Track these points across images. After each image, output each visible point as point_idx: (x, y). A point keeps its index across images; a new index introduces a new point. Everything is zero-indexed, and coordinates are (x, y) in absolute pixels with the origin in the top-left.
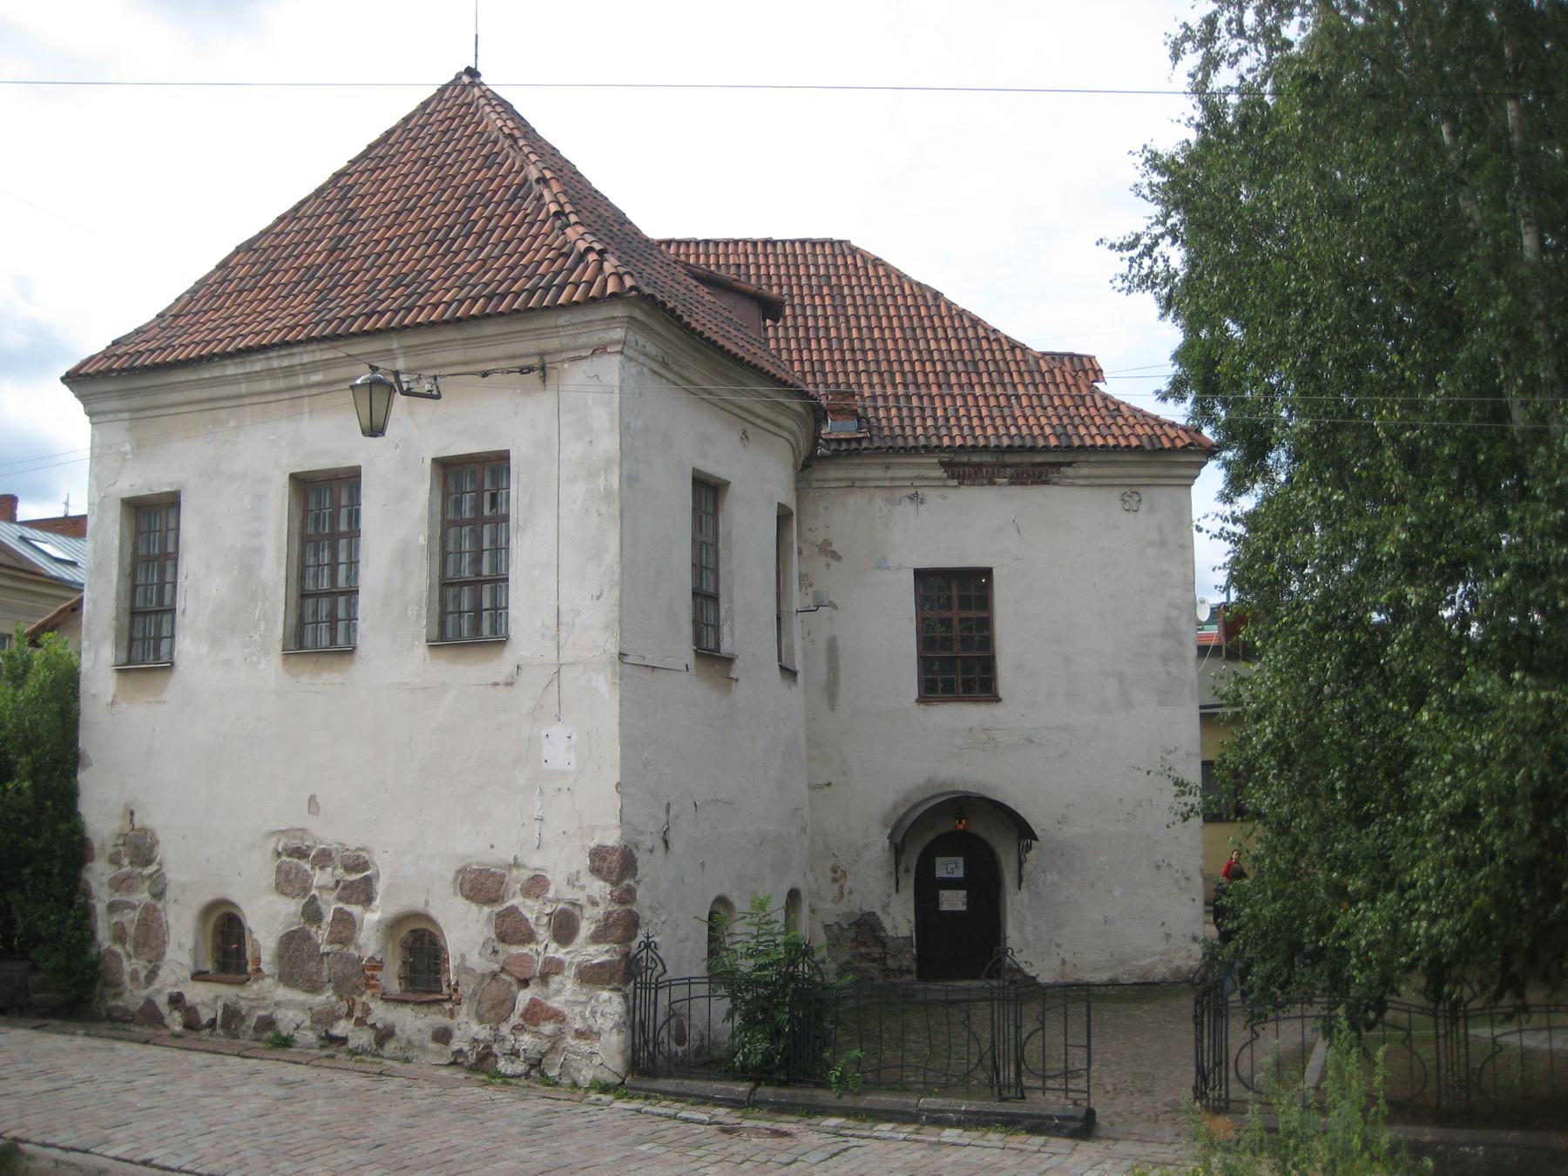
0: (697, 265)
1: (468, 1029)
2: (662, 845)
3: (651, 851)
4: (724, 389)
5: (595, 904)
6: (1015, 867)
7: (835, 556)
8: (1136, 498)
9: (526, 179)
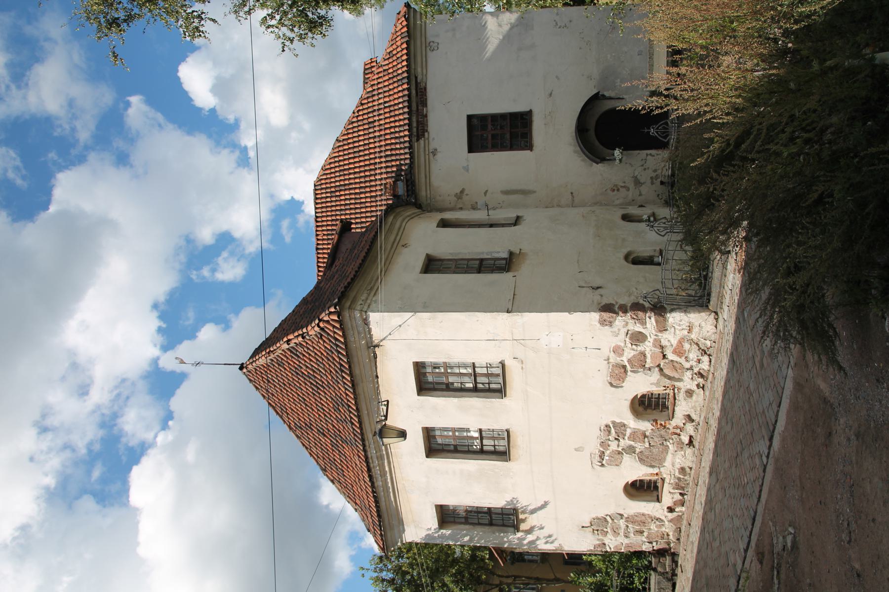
0: (327, 263)
1: (688, 382)
2: (599, 290)
3: (602, 296)
4: (381, 257)
5: (627, 324)
6: (613, 101)
7: (462, 192)
9: (288, 349)
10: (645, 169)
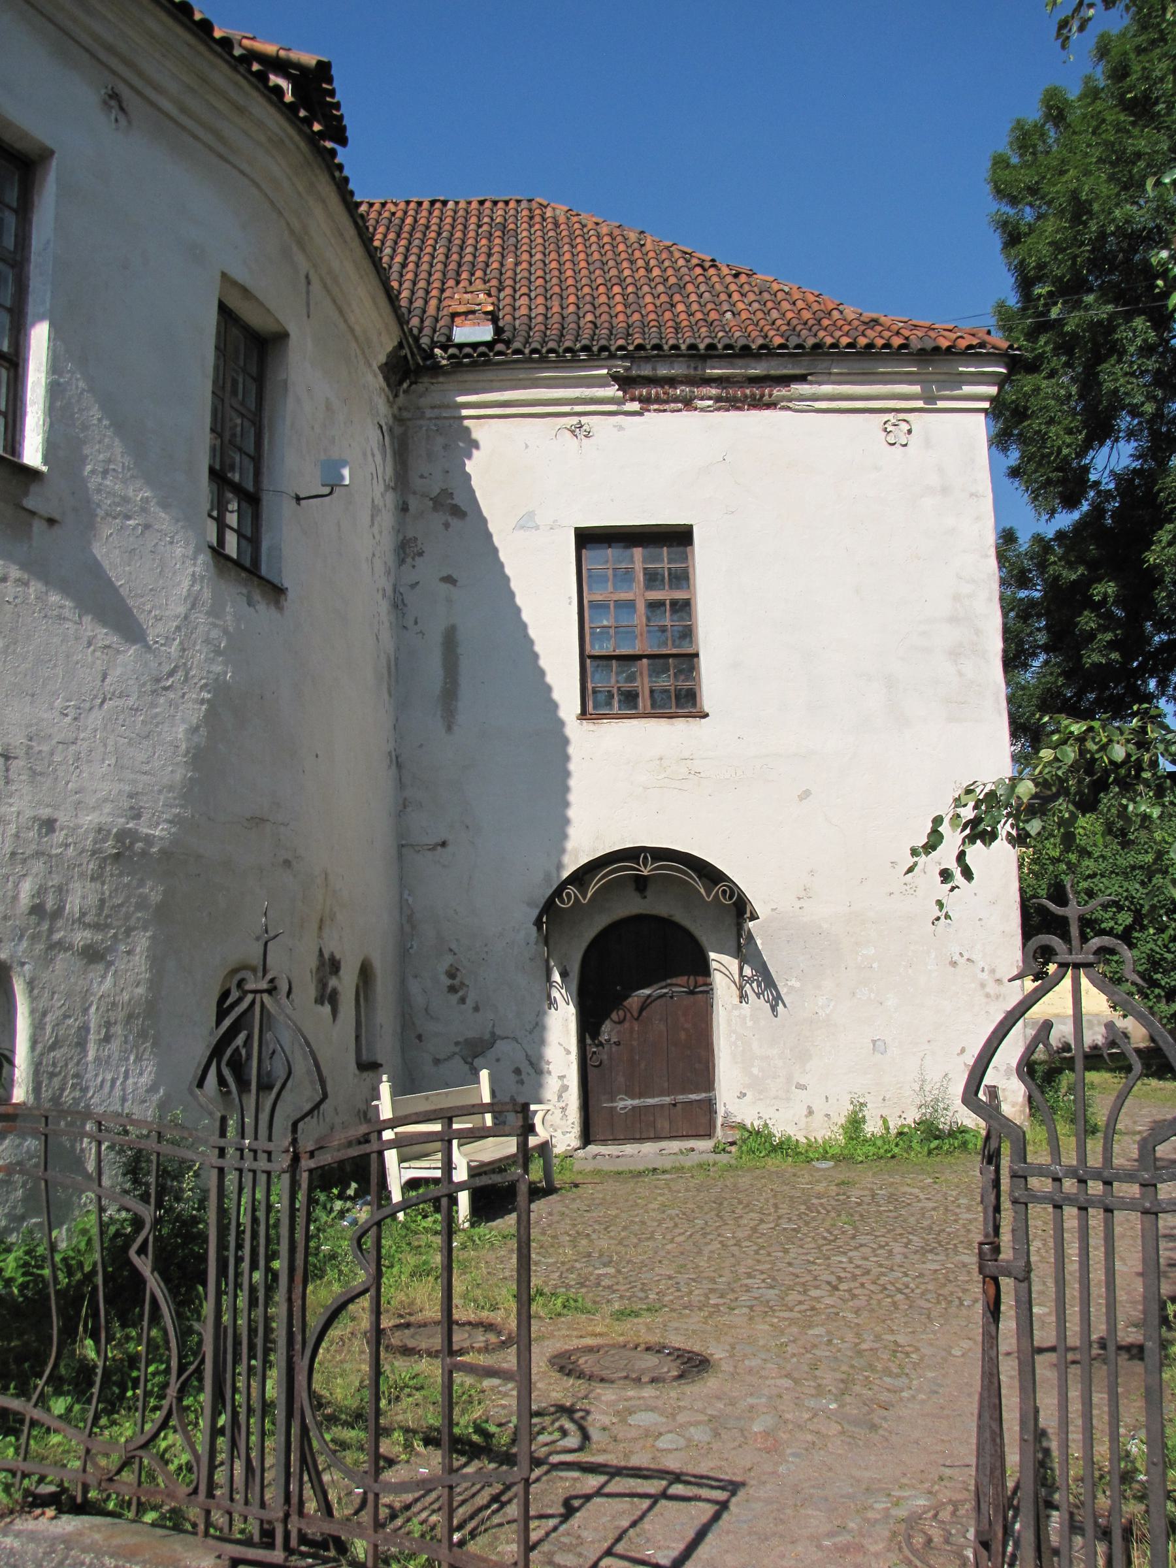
8: (904, 427)
10: (518, 1071)
